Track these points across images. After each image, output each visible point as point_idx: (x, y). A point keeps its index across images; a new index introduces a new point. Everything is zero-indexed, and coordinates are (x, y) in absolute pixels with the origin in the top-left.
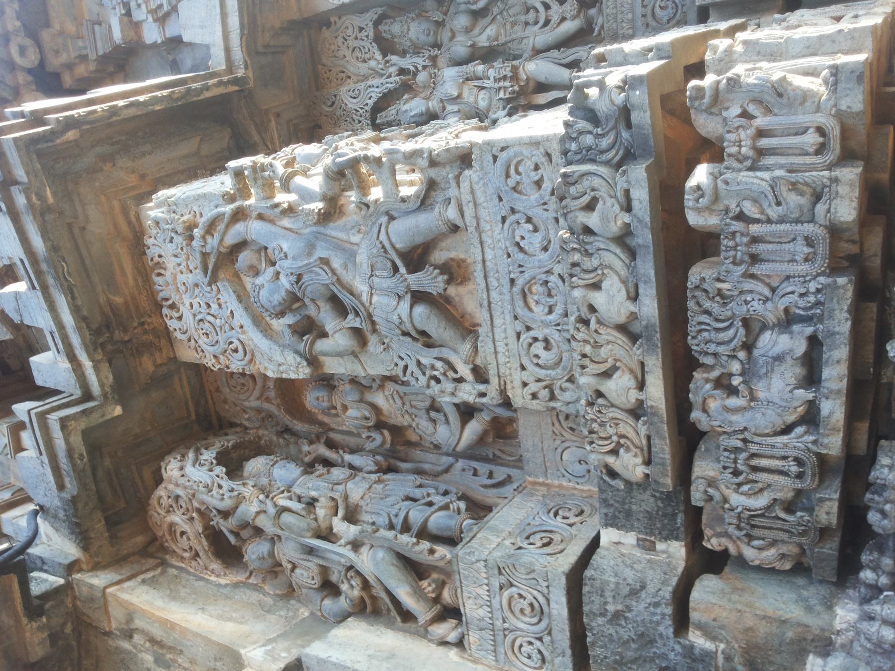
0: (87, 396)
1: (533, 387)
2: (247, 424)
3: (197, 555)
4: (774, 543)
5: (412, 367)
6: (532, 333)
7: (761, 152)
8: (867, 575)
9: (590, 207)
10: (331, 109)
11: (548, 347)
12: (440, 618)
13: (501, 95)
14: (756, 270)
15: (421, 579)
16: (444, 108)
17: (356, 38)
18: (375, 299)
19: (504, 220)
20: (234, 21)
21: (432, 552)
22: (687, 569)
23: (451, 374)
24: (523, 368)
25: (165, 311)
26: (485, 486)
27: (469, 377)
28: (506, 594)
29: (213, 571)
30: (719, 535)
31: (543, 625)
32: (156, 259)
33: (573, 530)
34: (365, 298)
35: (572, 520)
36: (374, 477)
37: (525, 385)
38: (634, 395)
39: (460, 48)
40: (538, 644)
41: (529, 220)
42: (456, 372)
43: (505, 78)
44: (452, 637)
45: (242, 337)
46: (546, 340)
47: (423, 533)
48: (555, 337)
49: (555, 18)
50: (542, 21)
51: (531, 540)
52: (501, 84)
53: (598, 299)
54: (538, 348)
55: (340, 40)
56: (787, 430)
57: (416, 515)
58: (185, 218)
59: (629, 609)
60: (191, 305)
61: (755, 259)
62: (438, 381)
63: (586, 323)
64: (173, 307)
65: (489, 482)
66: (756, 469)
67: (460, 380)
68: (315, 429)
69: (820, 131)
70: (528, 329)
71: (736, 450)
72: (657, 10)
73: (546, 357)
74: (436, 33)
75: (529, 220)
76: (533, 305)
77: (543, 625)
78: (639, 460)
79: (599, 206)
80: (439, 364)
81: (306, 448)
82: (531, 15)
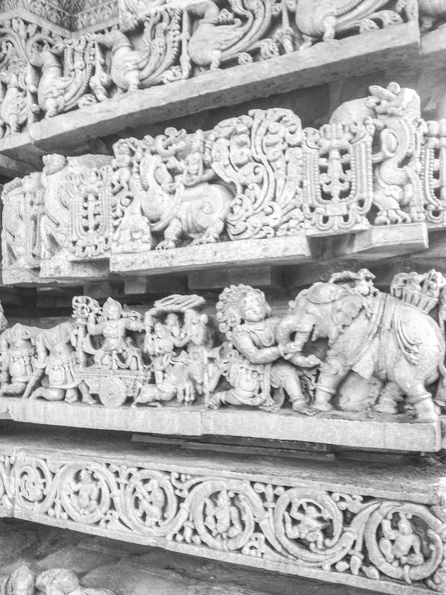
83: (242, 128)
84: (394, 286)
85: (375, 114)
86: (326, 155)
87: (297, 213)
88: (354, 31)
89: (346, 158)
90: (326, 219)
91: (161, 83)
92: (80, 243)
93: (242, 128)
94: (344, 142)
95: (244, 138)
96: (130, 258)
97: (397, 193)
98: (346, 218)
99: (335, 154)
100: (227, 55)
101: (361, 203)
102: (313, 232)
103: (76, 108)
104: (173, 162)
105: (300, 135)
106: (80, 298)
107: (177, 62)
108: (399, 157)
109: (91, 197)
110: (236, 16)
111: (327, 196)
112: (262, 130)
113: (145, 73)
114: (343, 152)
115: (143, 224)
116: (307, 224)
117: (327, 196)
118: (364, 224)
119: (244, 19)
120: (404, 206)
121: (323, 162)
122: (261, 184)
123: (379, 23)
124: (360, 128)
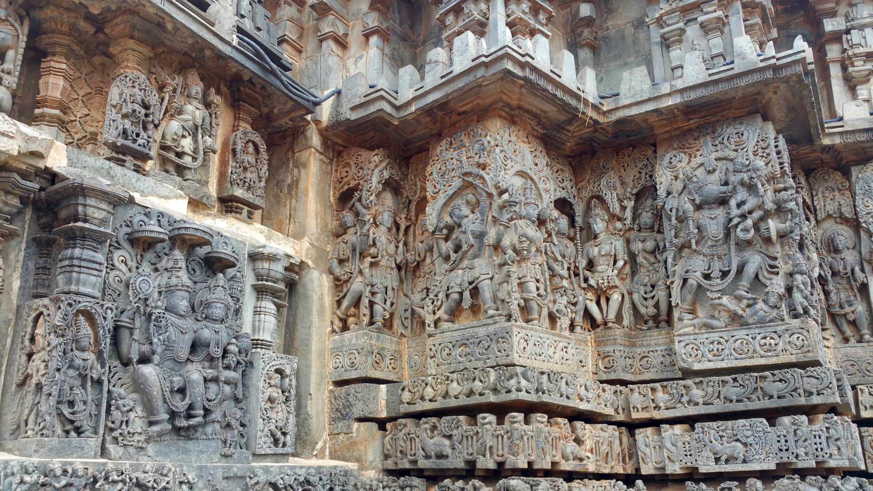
0: (398, 108)
1: (434, 348)
2: (409, 176)
3: (340, 182)
4: (392, 447)
5: (437, 290)
6: (452, 348)
7: (497, 437)
8: (386, 478)
9: (481, 381)
10: (601, 166)
11: (449, 355)
12: (341, 319)
13: (601, 281)
14: (464, 438)
15: (354, 307)
16: (596, 246)
17: (646, 174)
18: (460, 272)
19: (488, 336)
20: (634, 111)
21: (364, 315)
22: (378, 418)
23: (436, 309)
24: (440, 344)
25: (449, 139)
26: (401, 317)
27: (436, 317)
28: (355, 352)
29: (334, 193)
30: (391, 427)
31: (348, 367)
32: (472, 133)
33: (386, 369)
34: (461, 266)
35: (390, 367)
36: (394, 265)
37: (434, 345)
38: (427, 398)
39: (637, 246)
40: (341, 366)
41: (489, 347)
42: (438, 310)
43: (609, 282)
44: (335, 328)
45: (441, 192)
46: (450, 354)
47: (372, 304)
48: (451, 358)
49: (646, 303)
50: (645, 296)
51: (378, 356)
52: (606, 281)
53: (455, 384)
54: (447, 351)
55: (645, 162)
56: (423, 450)
57: (378, 298)
58: (488, 161)
59: (359, 401)
60: (452, 159)
61: (467, 437)
62: (433, 303)
63: (447, 380)
64: (451, 143)
65: (403, 318)
66: (411, 440)
67: (434, 313)
68: (413, 218)
69: (502, 456)
70: (453, 346)
71: (415, 434)
72: (646, 359)
73: (445, 353)
74: (646, 229)
75: (489, 347)
76: (461, 348)
77: (348, 367)
78: (408, 401)
79: (481, 384)
80: (439, 302)
81: (403, 216)
82: (649, 289)
83: (747, 424)
84: (807, 480)
85: (793, 424)
86: (779, 436)
87: (771, 455)
88: (784, 397)
89: (786, 438)
90: (781, 458)
91: (713, 404)
92: (684, 460)
93: (747, 424)
94: (785, 433)
95: (748, 428)
96: (707, 467)
97: (804, 450)
98: (788, 458)
99: (782, 437)
100: (740, 398)
101: (793, 453)
102: (778, 462)
103: (675, 408)
104: (721, 433)
105: (769, 429)
106: (689, 482)
107: (718, 397)
108: (803, 439)
109: (687, 443)
110: (741, 385)
111: (781, 450)
112: (755, 426)
113: (706, 399)
114: (785, 436)
115: (711, 455)
116: (775, 459)
117: (781, 450)
118: (795, 460)
119: (743, 386)
120: (806, 454)
121: (778, 439)
122: (757, 444)
123: (792, 395)
124: (789, 429)
